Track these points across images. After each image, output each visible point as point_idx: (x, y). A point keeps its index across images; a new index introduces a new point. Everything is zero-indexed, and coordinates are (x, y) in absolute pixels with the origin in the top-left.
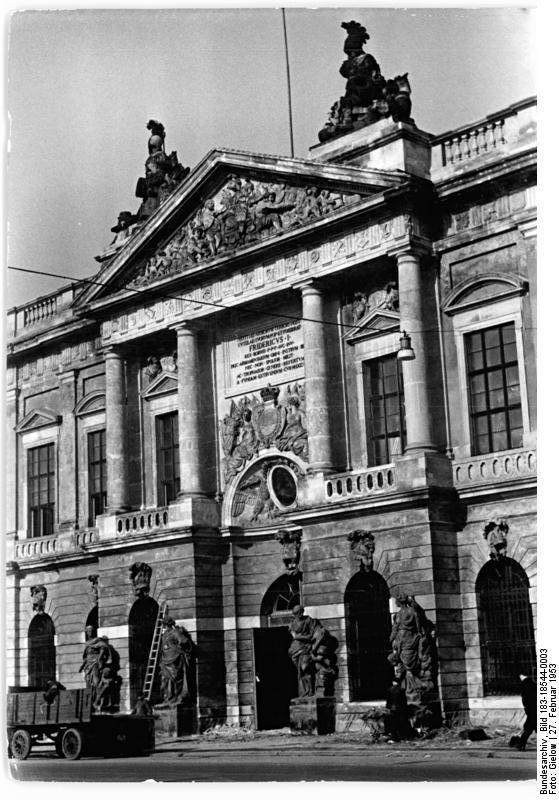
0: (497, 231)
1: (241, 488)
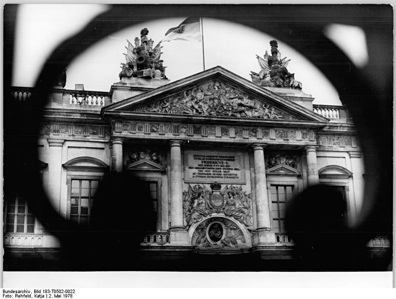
0: (339, 150)
1: (197, 229)
